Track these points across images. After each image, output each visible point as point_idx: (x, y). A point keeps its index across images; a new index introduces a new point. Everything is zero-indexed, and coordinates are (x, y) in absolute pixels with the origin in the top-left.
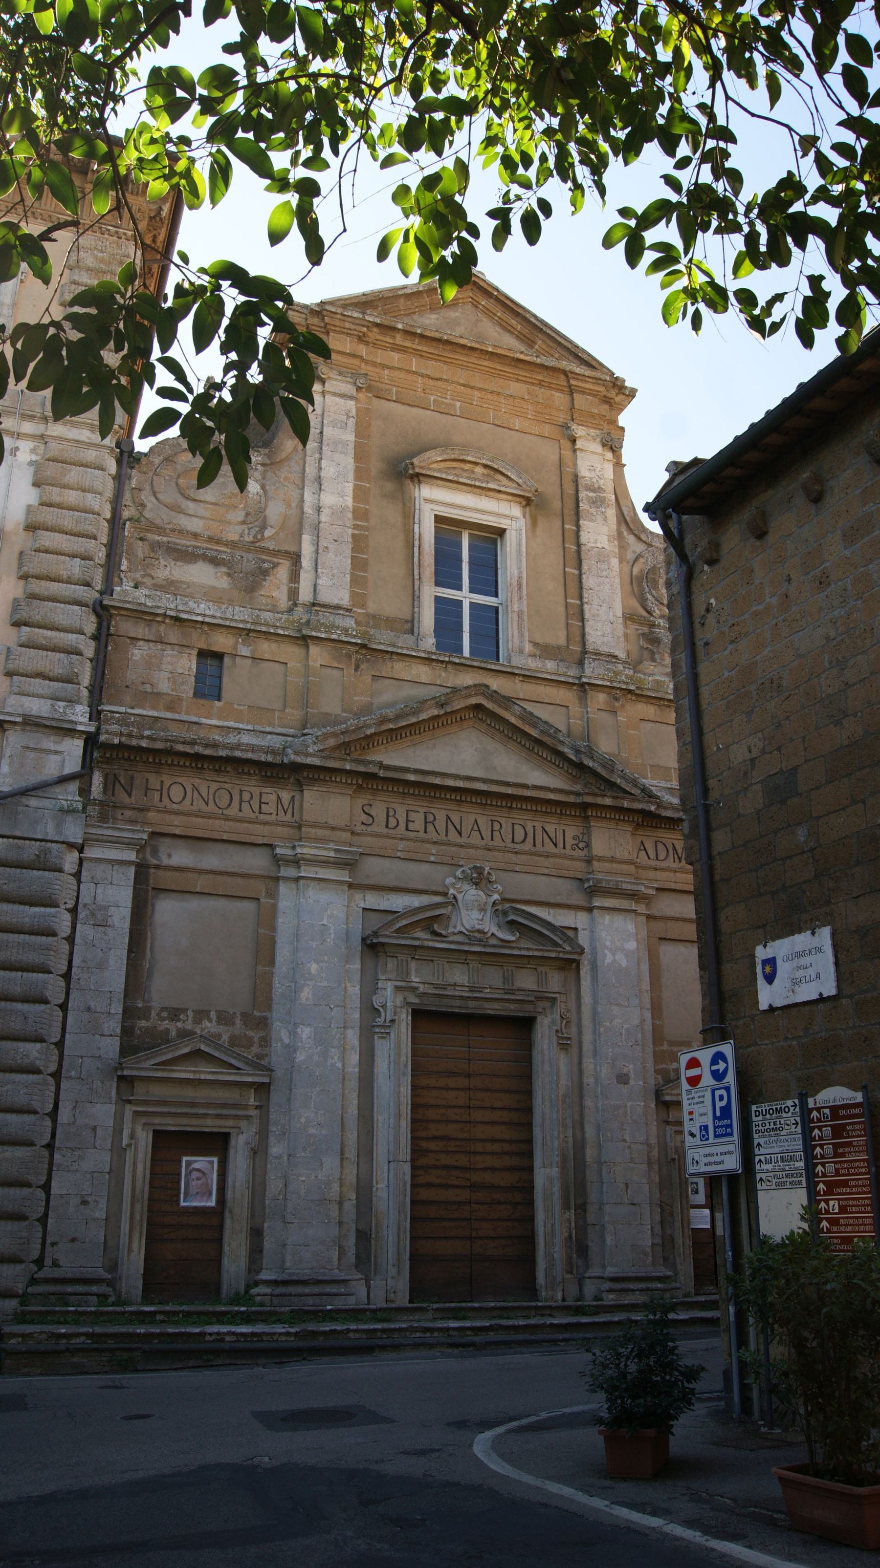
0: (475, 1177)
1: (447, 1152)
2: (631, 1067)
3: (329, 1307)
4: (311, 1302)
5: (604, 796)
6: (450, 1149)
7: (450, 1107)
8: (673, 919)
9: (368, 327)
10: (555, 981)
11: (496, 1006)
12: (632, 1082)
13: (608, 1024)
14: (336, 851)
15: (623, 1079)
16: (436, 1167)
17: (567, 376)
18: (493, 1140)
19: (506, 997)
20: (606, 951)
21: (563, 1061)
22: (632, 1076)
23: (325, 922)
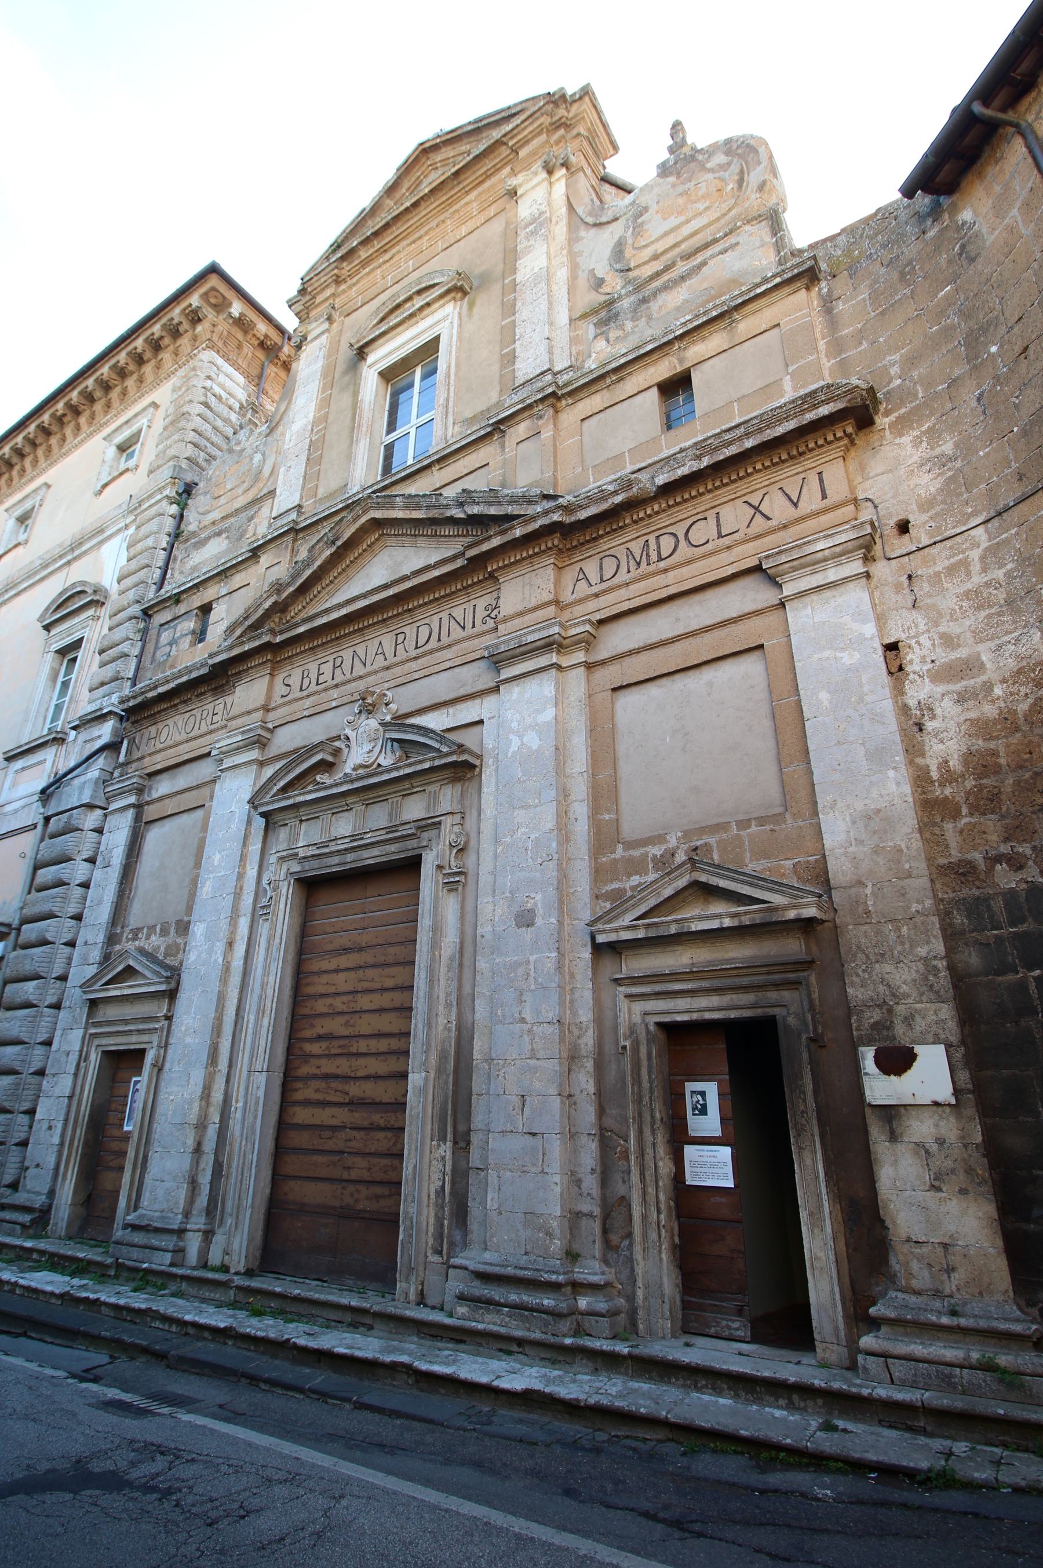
0: (355, 1090)
1: (330, 1056)
2: (539, 897)
3: (145, 1265)
4: (135, 1256)
5: (489, 538)
6: (333, 1051)
7: (339, 994)
8: (631, 653)
9: (336, 267)
10: (447, 797)
11: (376, 852)
12: (539, 921)
13: (508, 839)
14: (243, 733)
15: (525, 919)
16: (315, 1077)
17: (505, 144)
18: (380, 1035)
19: (390, 836)
20: (511, 736)
21: (450, 905)
22: (540, 911)
23: (232, 809)
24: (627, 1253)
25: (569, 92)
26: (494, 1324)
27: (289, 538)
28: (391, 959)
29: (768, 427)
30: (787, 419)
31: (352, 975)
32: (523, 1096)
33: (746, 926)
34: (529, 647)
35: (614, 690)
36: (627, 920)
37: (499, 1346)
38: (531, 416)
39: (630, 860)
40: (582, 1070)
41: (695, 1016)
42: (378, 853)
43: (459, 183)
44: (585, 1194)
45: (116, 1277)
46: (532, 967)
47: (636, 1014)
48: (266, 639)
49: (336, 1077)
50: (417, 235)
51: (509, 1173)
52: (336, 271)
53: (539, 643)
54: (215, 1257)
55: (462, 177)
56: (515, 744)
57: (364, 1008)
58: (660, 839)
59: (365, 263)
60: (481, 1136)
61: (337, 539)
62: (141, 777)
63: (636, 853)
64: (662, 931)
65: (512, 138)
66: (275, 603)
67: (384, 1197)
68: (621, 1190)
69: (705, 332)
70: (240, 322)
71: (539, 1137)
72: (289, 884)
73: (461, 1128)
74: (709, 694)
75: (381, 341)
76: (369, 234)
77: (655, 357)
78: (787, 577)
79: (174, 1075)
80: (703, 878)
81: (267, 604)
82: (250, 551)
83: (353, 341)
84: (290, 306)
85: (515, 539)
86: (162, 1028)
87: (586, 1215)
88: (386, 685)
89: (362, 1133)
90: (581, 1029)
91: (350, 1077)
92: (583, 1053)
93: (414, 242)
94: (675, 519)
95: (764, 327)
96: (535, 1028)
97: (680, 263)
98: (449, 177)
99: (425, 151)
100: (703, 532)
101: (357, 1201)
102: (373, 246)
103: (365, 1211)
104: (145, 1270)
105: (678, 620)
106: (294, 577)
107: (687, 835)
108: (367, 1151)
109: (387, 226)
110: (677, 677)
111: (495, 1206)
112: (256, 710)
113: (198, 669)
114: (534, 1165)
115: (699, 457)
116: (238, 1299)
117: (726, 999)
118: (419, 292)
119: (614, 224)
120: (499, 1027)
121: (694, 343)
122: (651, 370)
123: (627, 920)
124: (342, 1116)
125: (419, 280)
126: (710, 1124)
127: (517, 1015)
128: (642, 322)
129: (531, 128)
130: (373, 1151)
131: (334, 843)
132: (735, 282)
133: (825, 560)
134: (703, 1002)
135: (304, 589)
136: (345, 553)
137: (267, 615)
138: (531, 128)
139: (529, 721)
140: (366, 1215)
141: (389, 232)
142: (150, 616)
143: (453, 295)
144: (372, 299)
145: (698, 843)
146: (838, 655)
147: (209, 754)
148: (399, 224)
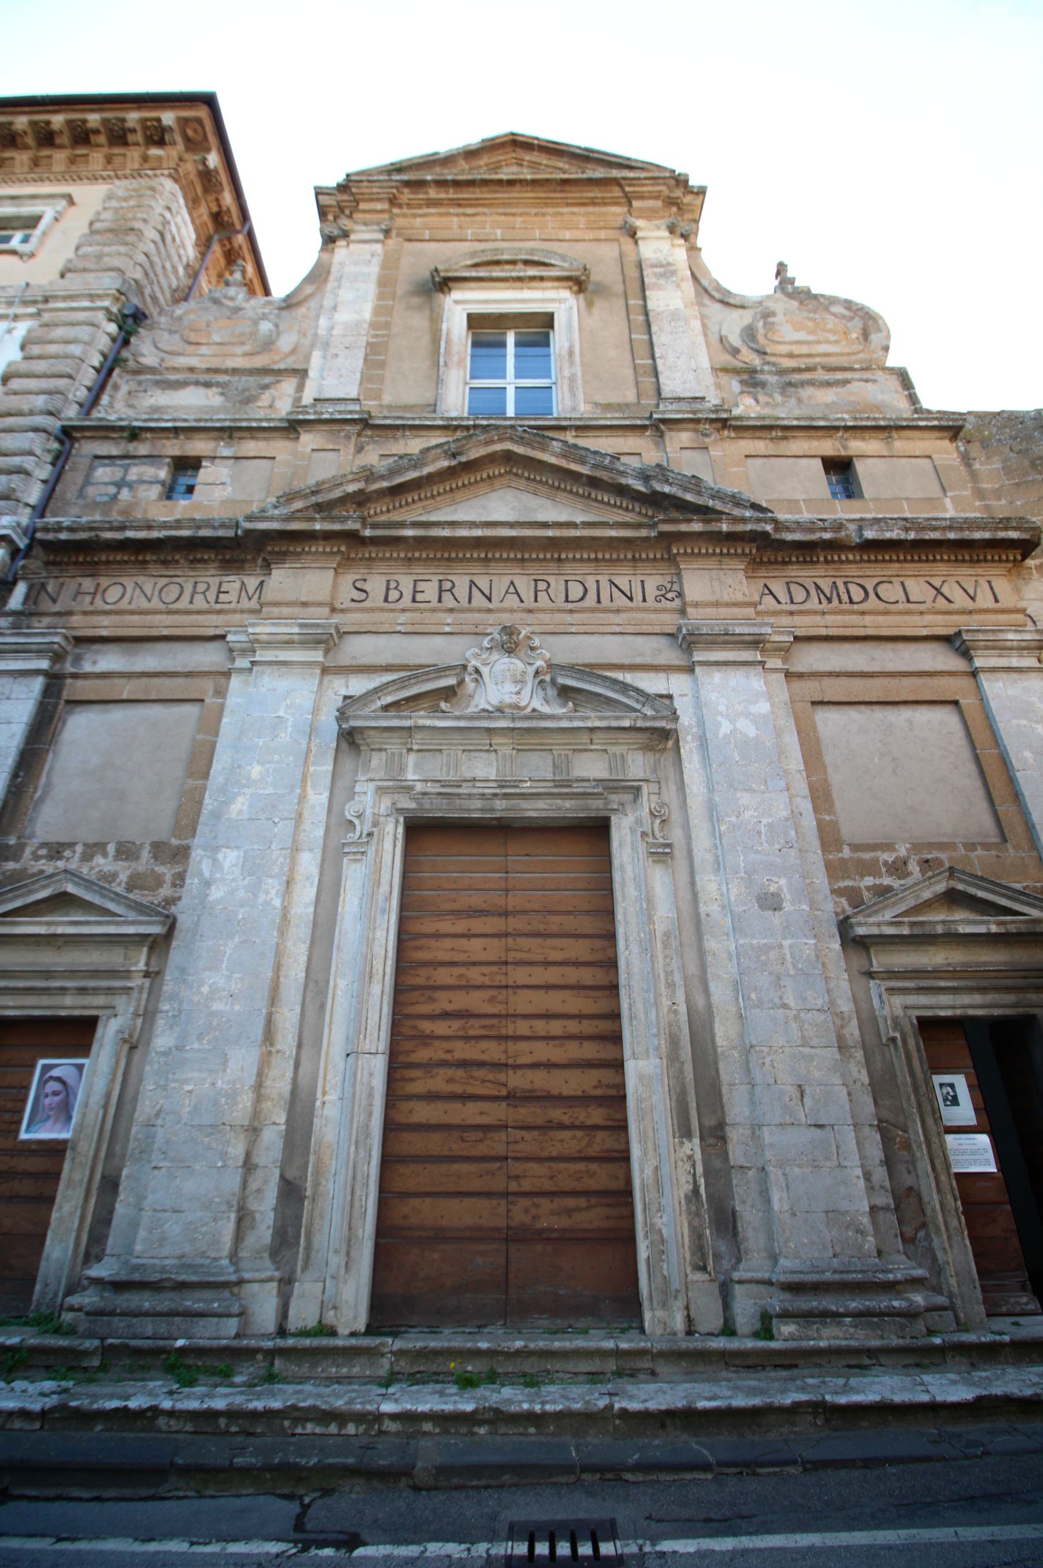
0: (517, 1080)
1: (467, 1038)
2: (783, 882)
3: (180, 1343)
4: (149, 1330)
5: (689, 521)
6: (471, 1033)
7: (474, 964)
8: (830, 674)
9: (397, 188)
10: (638, 765)
11: (541, 804)
12: (787, 907)
13: (733, 819)
14: (301, 626)
15: (771, 902)
16: (444, 1064)
17: (620, 186)
18: (548, 1016)
19: (556, 790)
20: (719, 718)
21: (659, 880)
22: (787, 896)
23: (281, 713)
24: (925, 1244)
25: (691, 183)
26: (834, 1338)
27: (354, 429)
28: (554, 928)
29: (968, 529)
30: (984, 529)
31: (495, 942)
32: (800, 1086)
33: (1012, 935)
34: (736, 638)
35: (813, 703)
36: (888, 915)
37: (844, 1362)
38: (695, 430)
39: (859, 862)
40: (852, 1061)
41: (958, 1012)
42: (544, 807)
43: (562, 191)
44: (877, 1187)
45: (103, 1368)
46: (787, 951)
47: (898, 1007)
48: (350, 525)
49: (482, 1064)
50: (514, 211)
51: (797, 1170)
52: (394, 191)
53: (747, 638)
54: (303, 1313)
55: (567, 188)
56: (726, 728)
57: (520, 983)
58: (889, 847)
59: (432, 203)
60: (741, 1131)
61: (460, 454)
62: (66, 638)
63: (867, 856)
64: (928, 930)
65: (630, 185)
66: (361, 491)
67: (579, 1209)
68: (909, 1181)
69: (867, 435)
70: (207, 176)
71: (828, 1128)
72: (397, 821)
73: (710, 1121)
74: (911, 730)
75: (473, 285)
76: (449, 178)
77: (820, 433)
78: (979, 653)
79: (190, 1055)
80: (960, 887)
81: (351, 488)
82: (289, 421)
83: (440, 267)
84: (317, 194)
85: (720, 532)
86: (141, 989)
87: (882, 1208)
88: (537, 629)
89: (535, 1133)
90: (843, 1019)
91: (506, 1065)
92: (850, 1042)
93: (505, 214)
94: (870, 574)
95: (917, 453)
96: (802, 1015)
97: (820, 371)
98: (555, 180)
99: (516, 144)
100: (891, 592)
101: (535, 1218)
102: (447, 193)
103: (551, 1230)
104: (181, 1350)
105: (873, 659)
106: (392, 472)
107: (916, 847)
108: (545, 1154)
109: (471, 183)
110: (875, 707)
111: (786, 1207)
112: (319, 604)
113: (214, 528)
114: (827, 1159)
115: (907, 530)
116: (397, 1369)
117: (989, 998)
118: (527, 263)
119: (740, 311)
120: (756, 1012)
121: (855, 438)
122: (815, 443)
123: (888, 915)
124: (498, 1112)
125: (532, 251)
126: (965, 1112)
127: (777, 1000)
128: (793, 401)
129: (650, 189)
130: (554, 1154)
131: (470, 784)
132: (877, 408)
133: (1011, 649)
134: (966, 999)
135: (396, 491)
136: (462, 473)
137: (343, 500)
138: (650, 189)
139: (740, 708)
140: (554, 1235)
141: (471, 189)
142: (73, 440)
143: (570, 284)
144: (444, 241)
145: (929, 856)
146: (1035, 726)
147: (223, 637)
148: (485, 189)
